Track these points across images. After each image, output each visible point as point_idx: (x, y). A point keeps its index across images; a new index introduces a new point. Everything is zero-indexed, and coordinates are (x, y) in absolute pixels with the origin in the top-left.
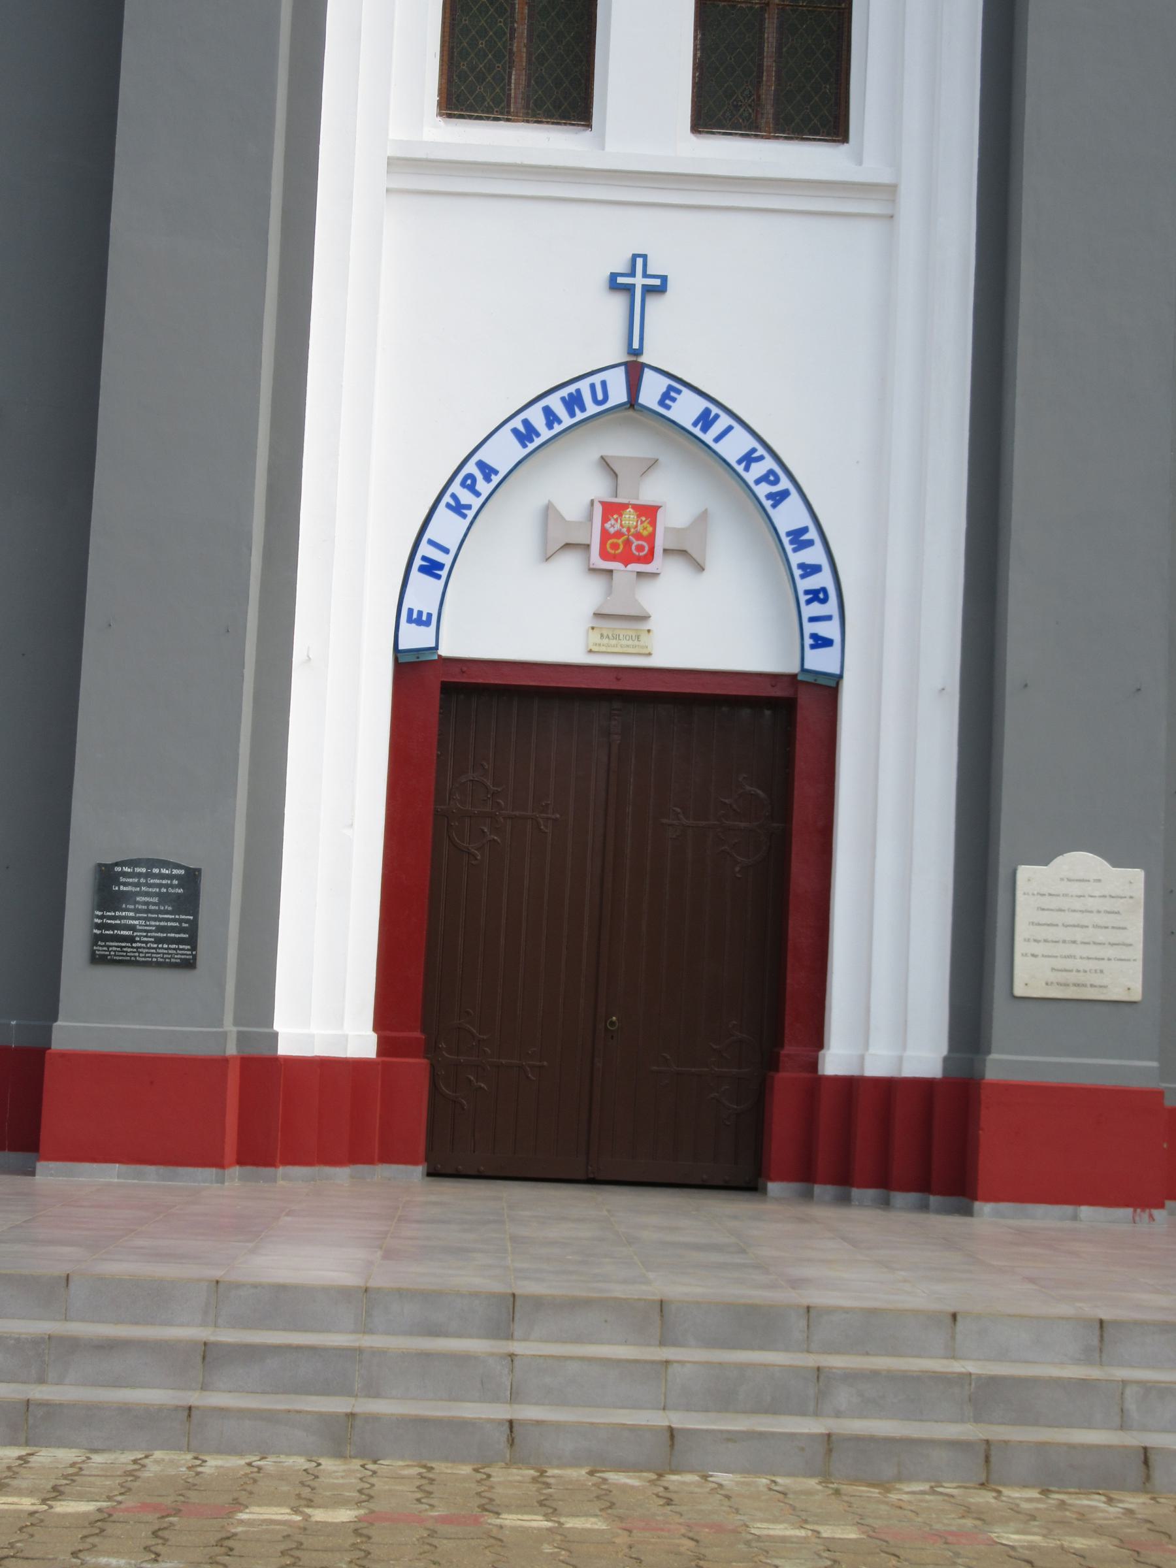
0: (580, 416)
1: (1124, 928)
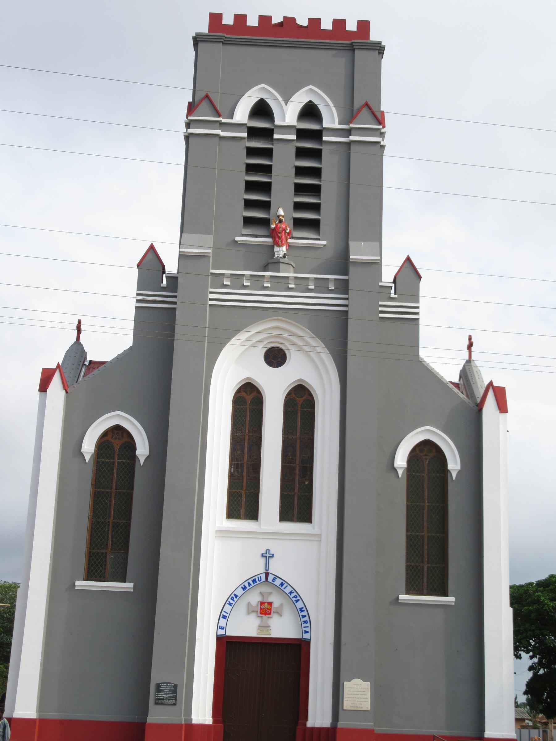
1: (366, 695)
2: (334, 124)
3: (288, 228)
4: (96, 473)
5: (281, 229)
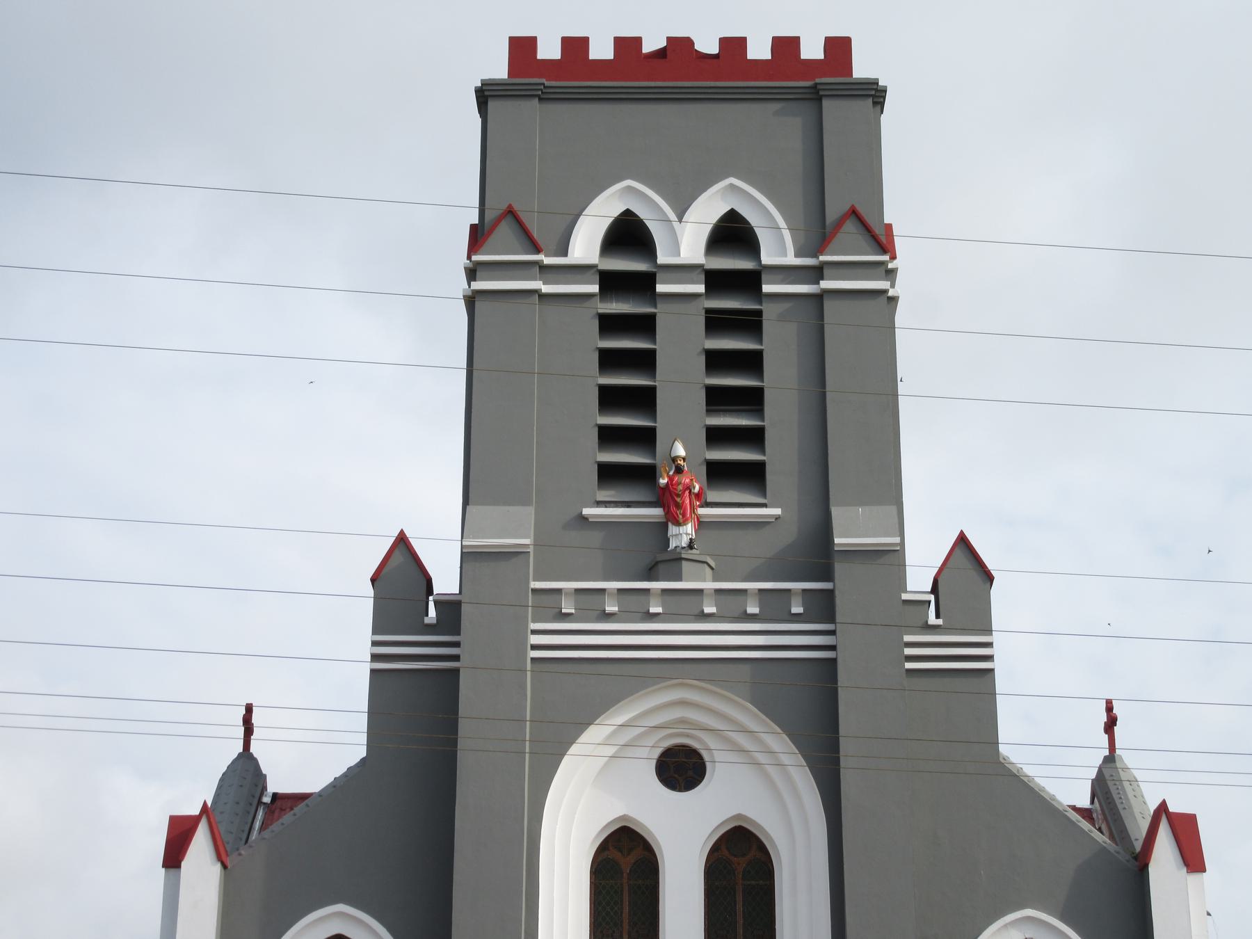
2: (786, 256)
3: (695, 483)
5: (680, 487)
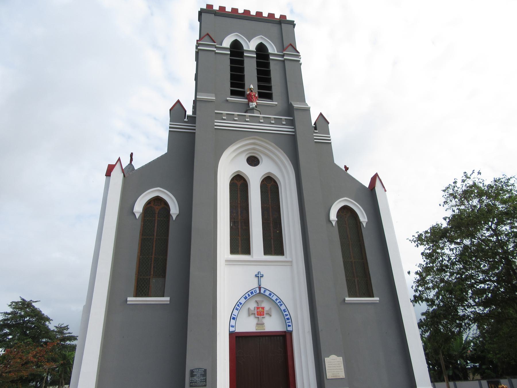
0: (253, 295)
2: (275, 52)
4: (143, 227)
